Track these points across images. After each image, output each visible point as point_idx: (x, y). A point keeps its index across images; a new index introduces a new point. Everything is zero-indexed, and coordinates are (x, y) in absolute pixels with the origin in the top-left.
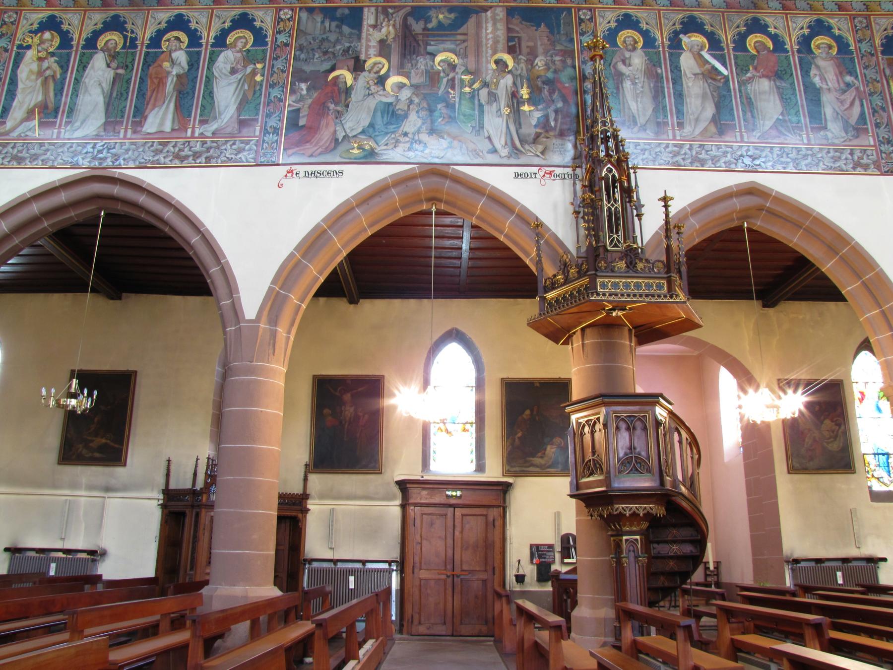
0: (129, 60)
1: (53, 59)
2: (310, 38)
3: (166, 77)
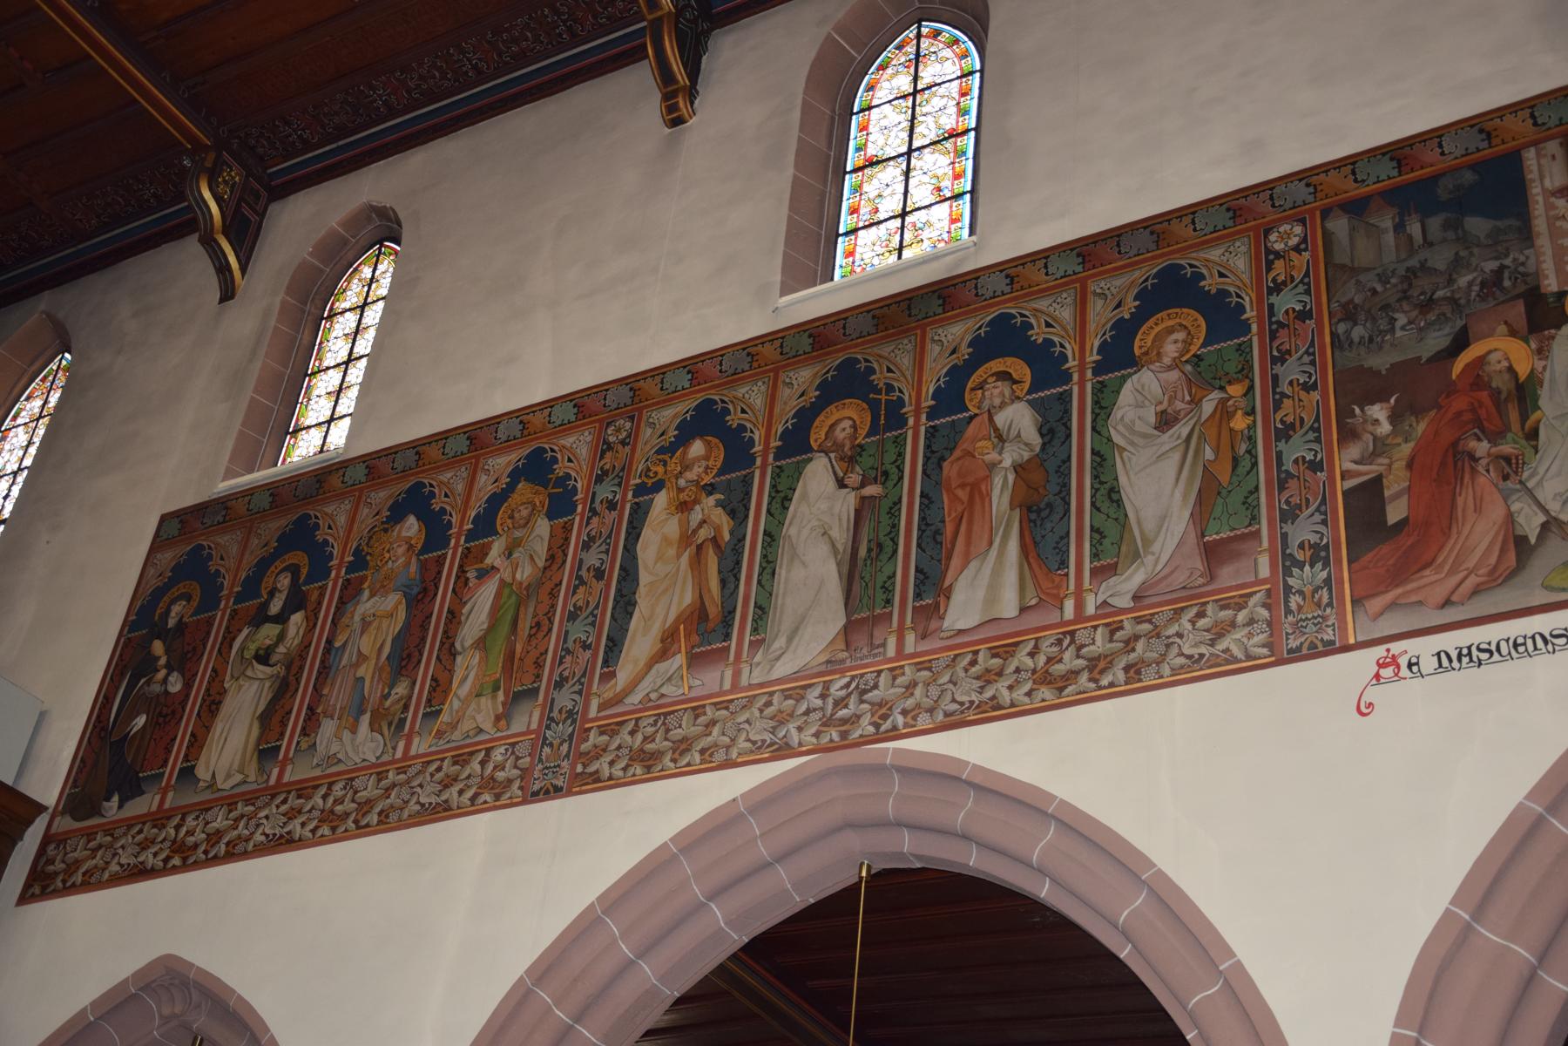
0: (890, 456)
1: (711, 501)
2: (1370, 280)
3: (988, 478)
